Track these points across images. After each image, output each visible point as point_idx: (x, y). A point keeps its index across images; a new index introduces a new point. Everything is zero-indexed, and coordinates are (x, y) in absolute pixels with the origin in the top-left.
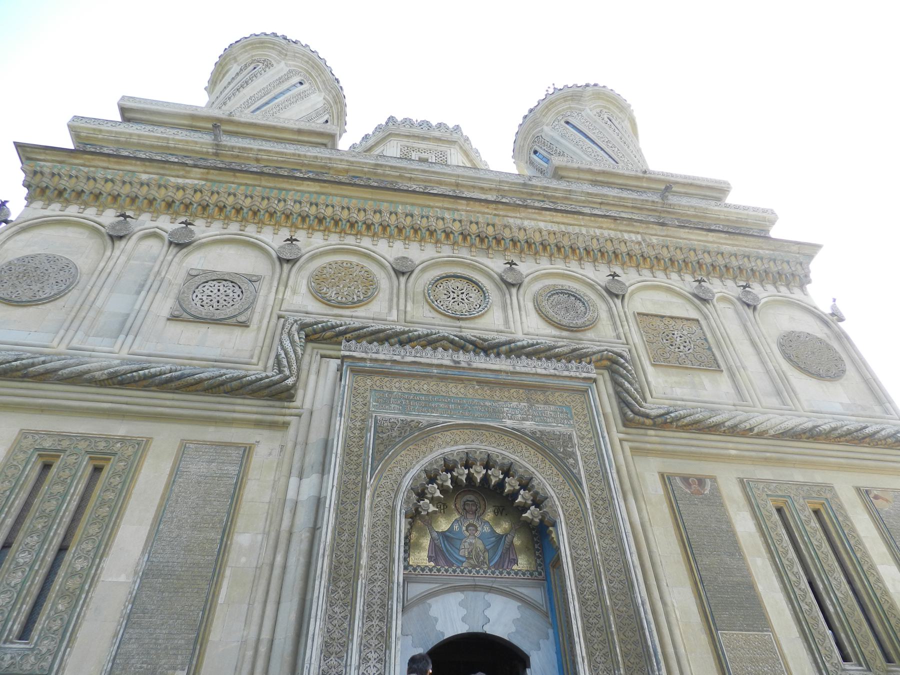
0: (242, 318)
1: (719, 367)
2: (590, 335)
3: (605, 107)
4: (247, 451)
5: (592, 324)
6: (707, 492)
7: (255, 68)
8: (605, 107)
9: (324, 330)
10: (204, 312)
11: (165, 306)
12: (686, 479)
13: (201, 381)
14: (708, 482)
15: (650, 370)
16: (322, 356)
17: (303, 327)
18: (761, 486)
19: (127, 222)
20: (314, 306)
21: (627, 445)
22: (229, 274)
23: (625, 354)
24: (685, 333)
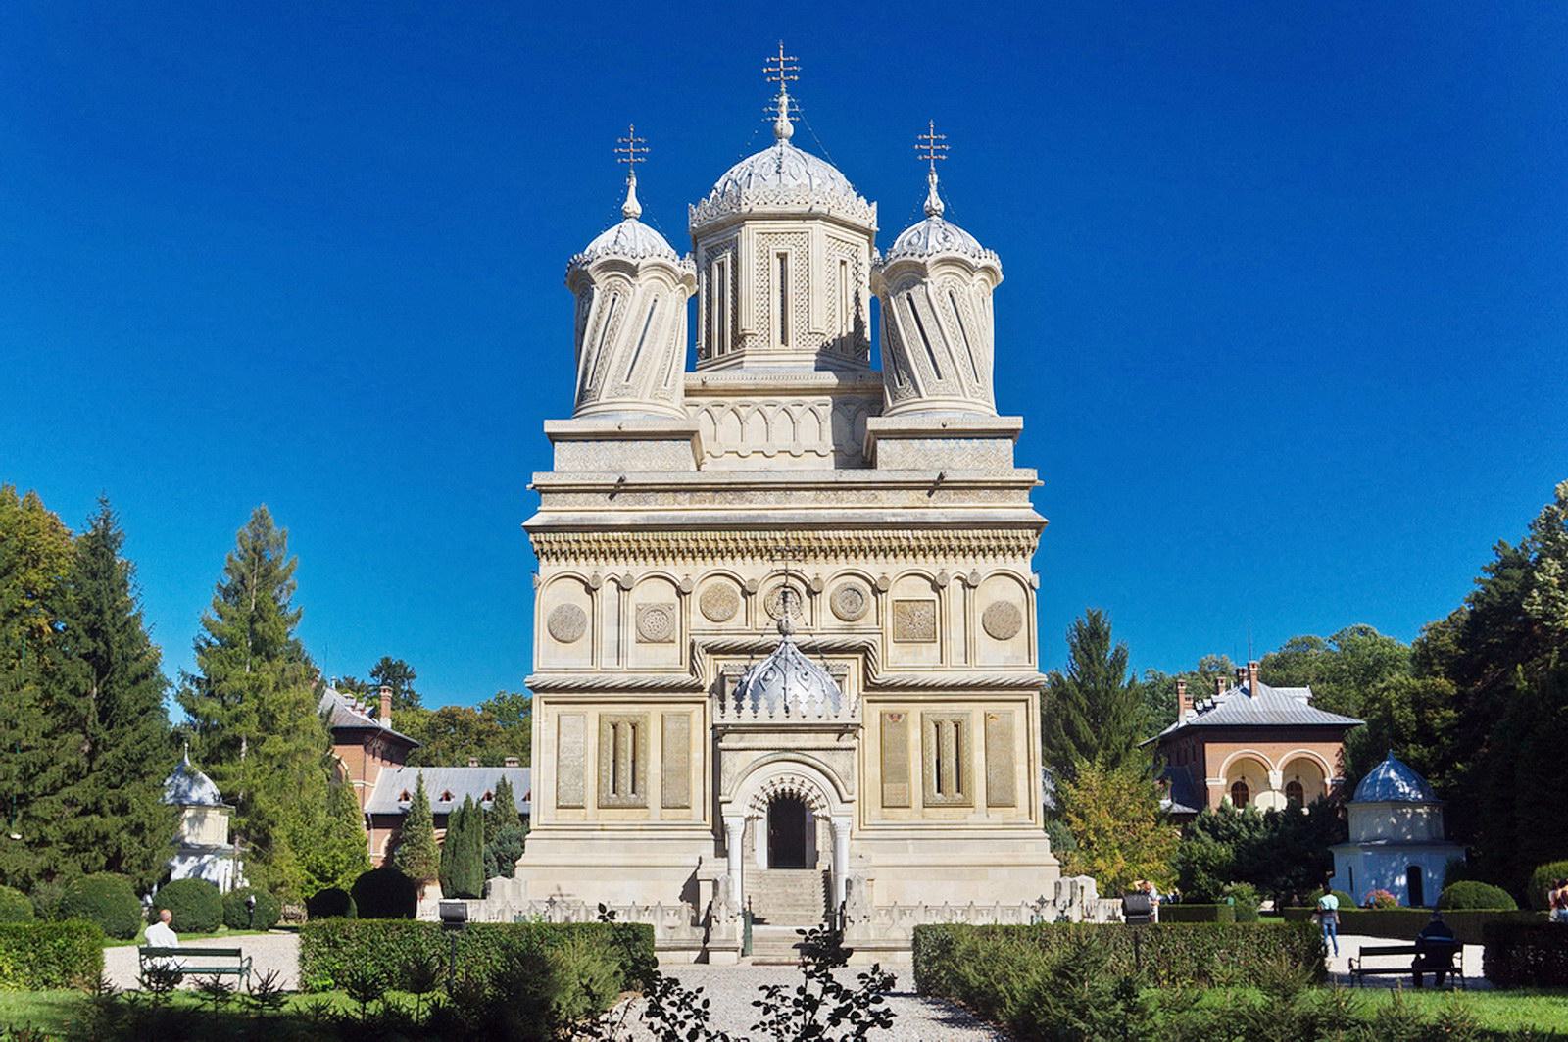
0: (672, 638)
1: (935, 638)
2: (861, 622)
3: (949, 273)
4: (688, 715)
5: (865, 613)
6: (900, 721)
7: (614, 300)
8: (949, 273)
9: (714, 647)
10: (652, 637)
11: (631, 634)
12: (891, 716)
13: (663, 686)
14: (903, 715)
15: (891, 645)
16: (715, 659)
17: (703, 647)
18: (930, 716)
19: (598, 576)
20: (707, 624)
21: (865, 698)
22: (657, 605)
23: (874, 643)
24: (923, 612)
